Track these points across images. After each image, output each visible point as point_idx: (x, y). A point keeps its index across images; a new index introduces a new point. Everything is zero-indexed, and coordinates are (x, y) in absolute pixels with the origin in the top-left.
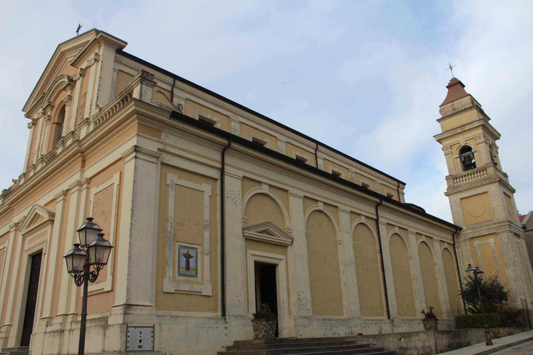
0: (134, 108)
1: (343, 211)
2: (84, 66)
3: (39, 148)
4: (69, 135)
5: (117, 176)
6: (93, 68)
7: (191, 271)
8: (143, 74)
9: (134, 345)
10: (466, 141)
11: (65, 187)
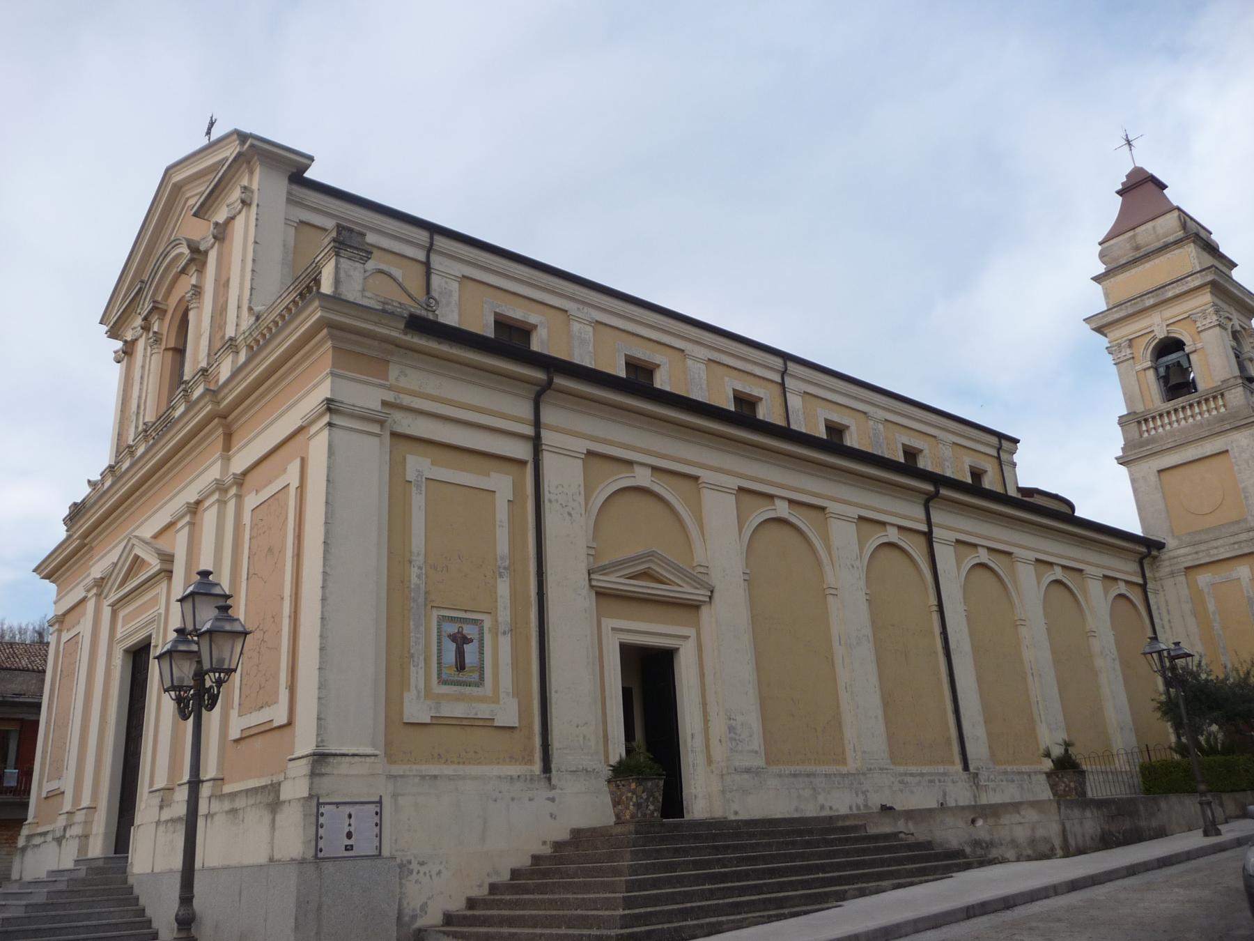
0: (319, 314)
1: (841, 517)
2: (221, 217)
3: (139, 407)
5: (294, 468)
6: (239, 222)
7: (470, 671)
8: (339, 233)
9: (334, 845)
10: (1168, 325)
11: (191, 495)
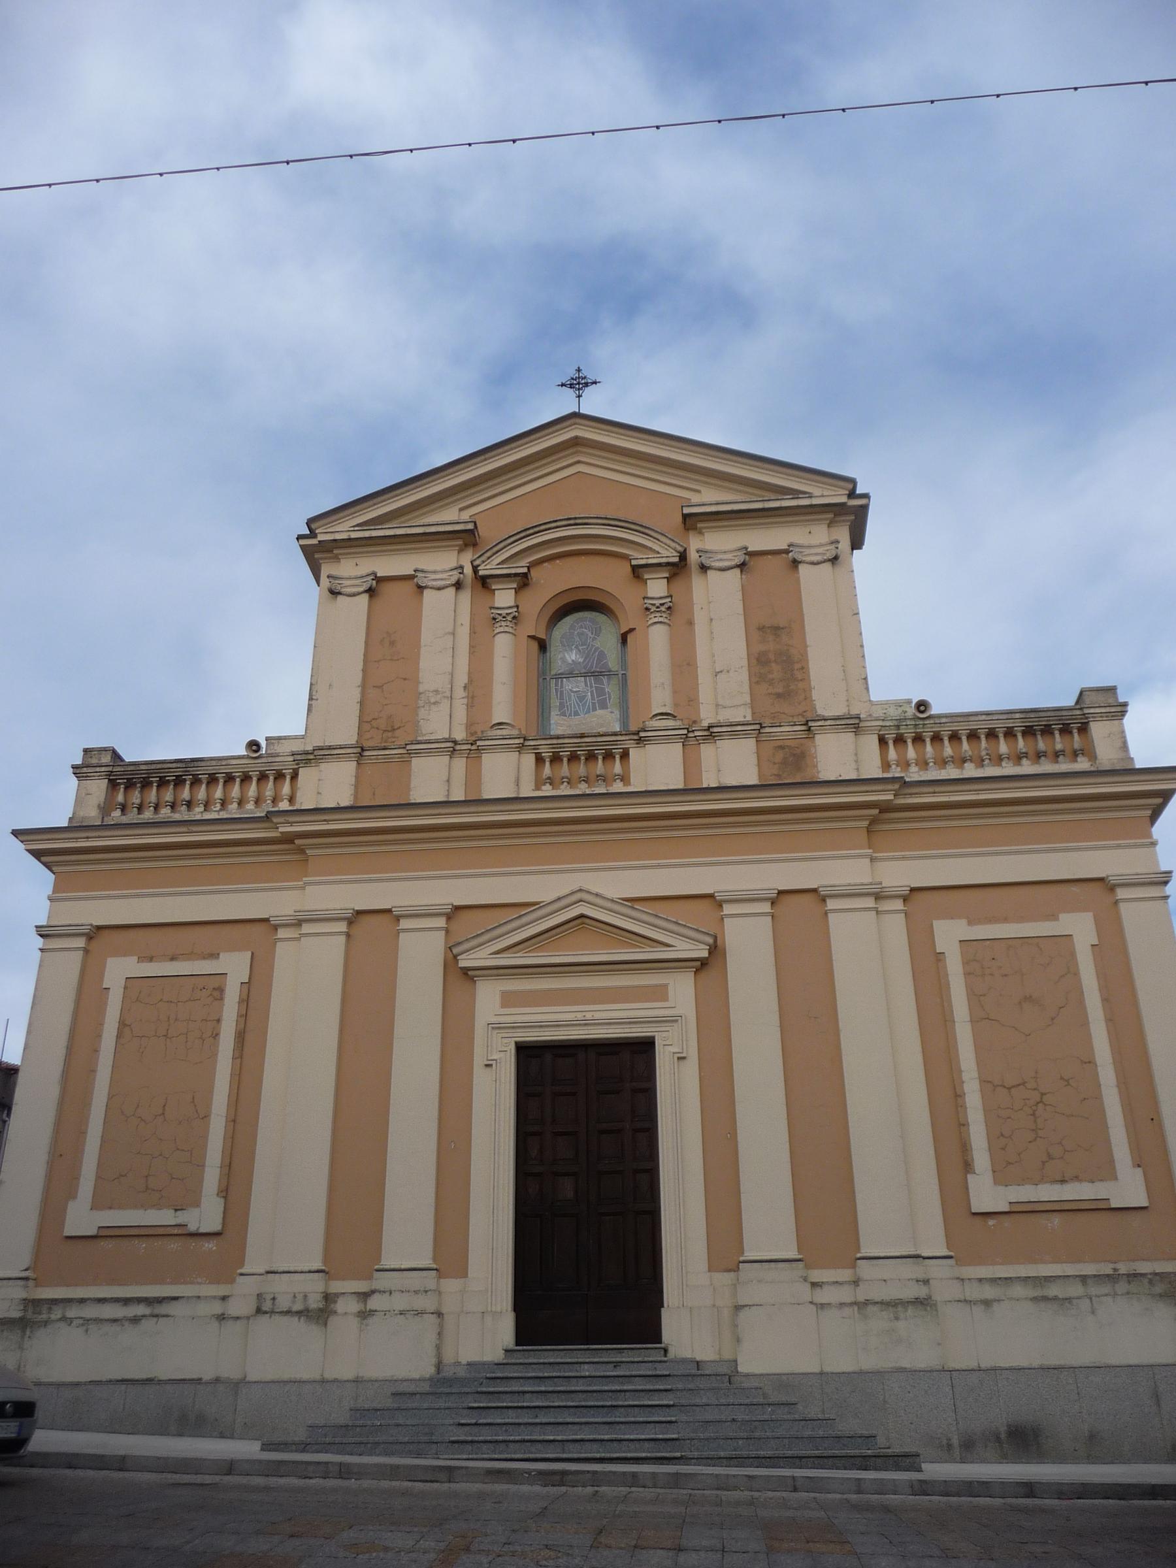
4: (739, 728)
